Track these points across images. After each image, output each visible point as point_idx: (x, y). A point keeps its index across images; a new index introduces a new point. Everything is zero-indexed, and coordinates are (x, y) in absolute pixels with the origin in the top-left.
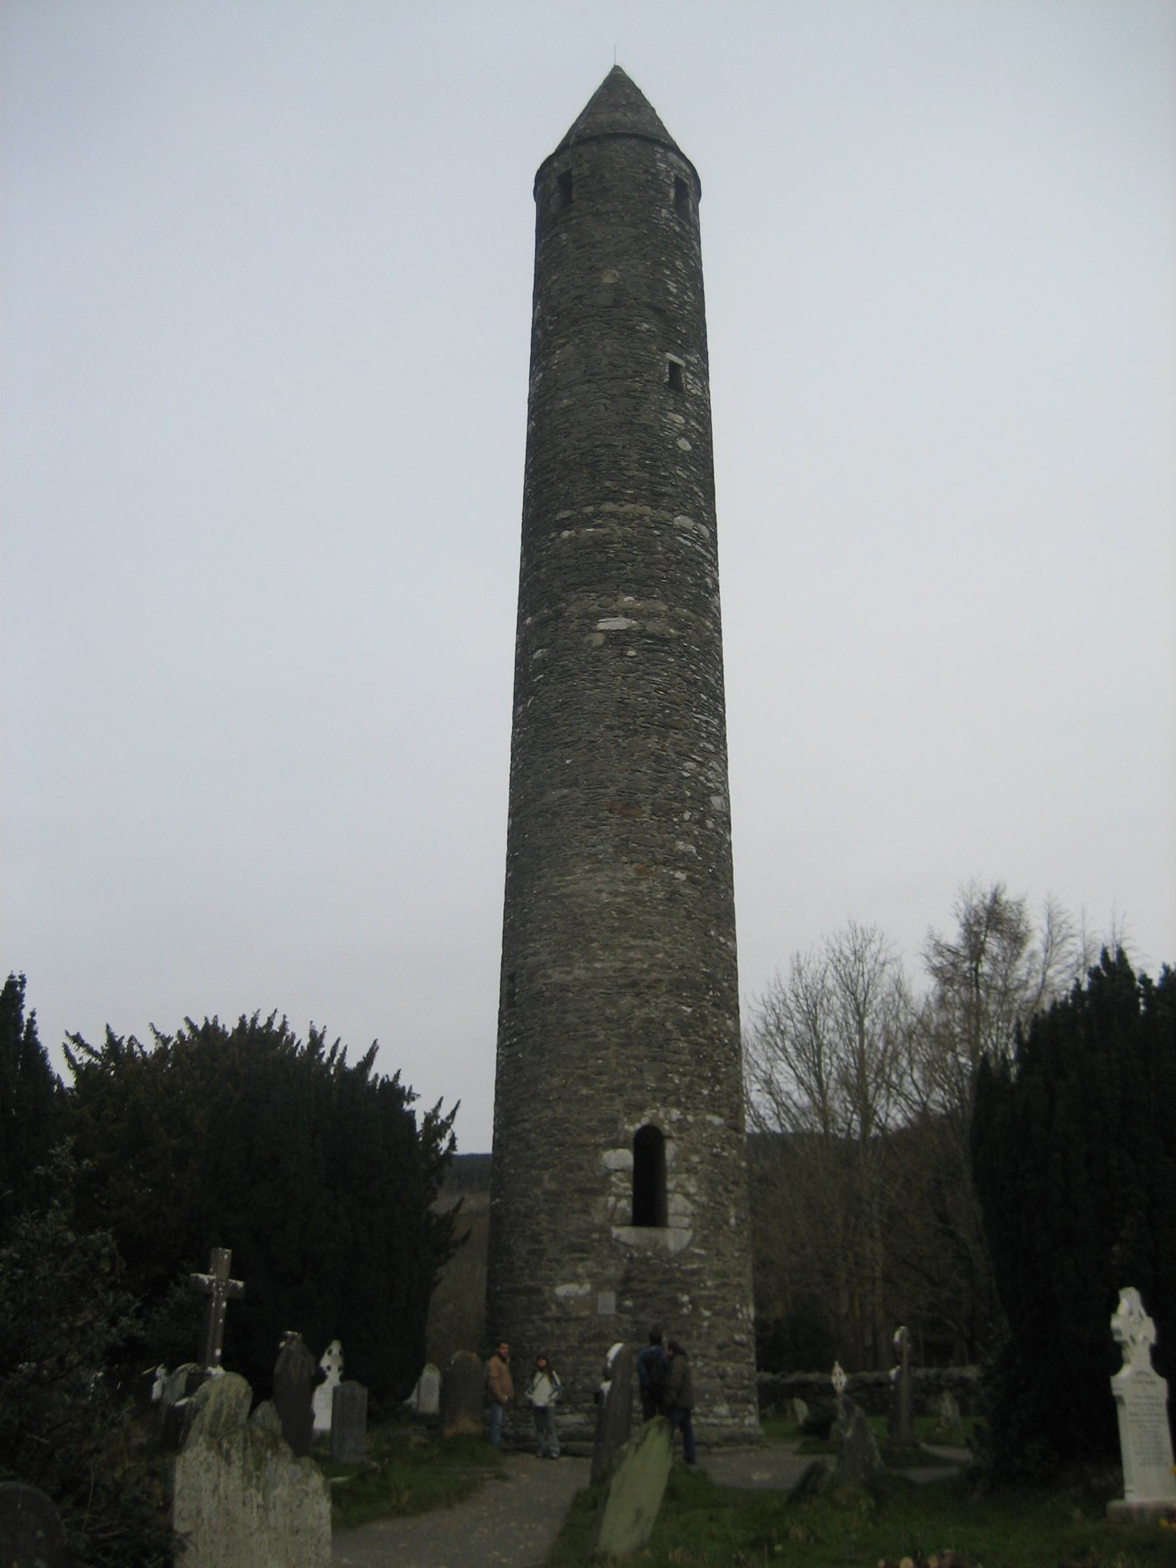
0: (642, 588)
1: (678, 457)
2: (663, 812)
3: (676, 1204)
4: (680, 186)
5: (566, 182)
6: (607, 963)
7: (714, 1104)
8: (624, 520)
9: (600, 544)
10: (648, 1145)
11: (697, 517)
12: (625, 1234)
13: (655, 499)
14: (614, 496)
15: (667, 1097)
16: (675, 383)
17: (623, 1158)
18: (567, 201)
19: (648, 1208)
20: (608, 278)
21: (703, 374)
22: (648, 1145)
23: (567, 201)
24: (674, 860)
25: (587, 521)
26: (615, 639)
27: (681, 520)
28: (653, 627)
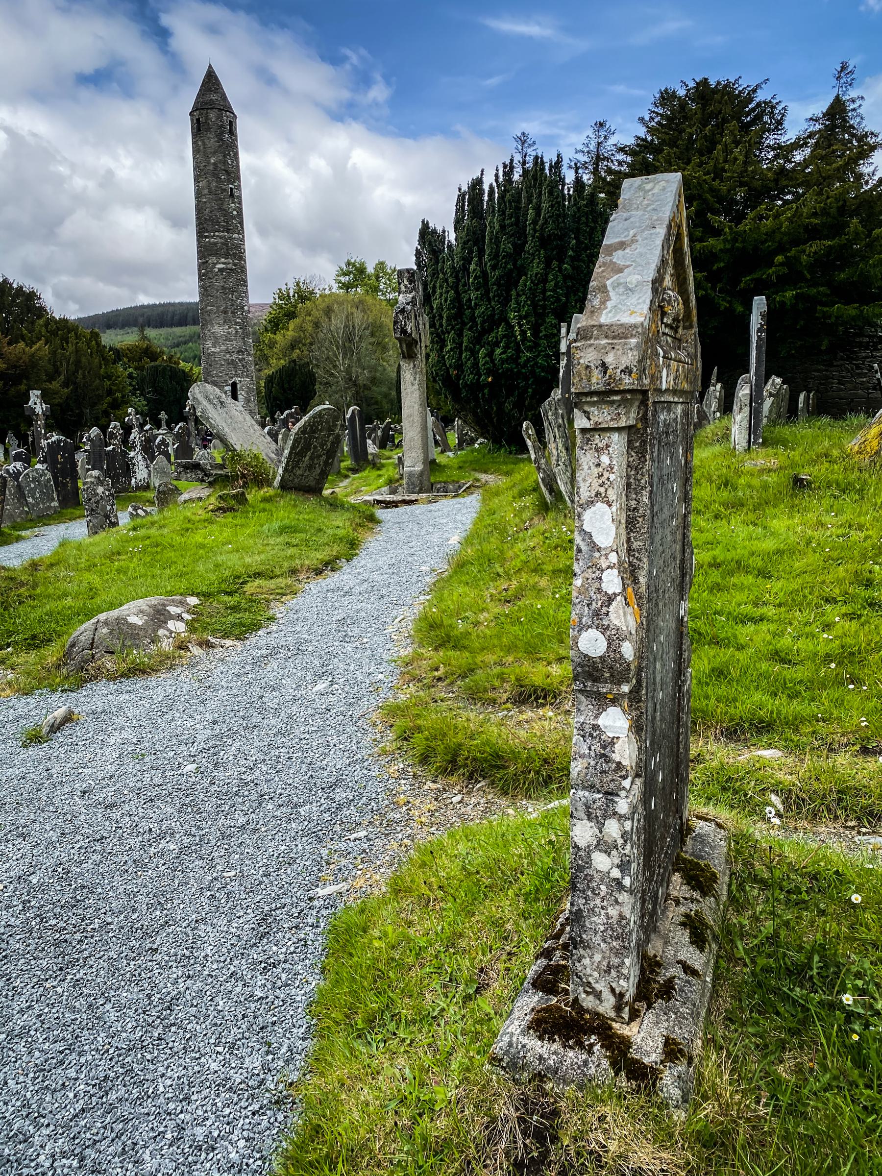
1: (233, 218)
2: (233, 313)
3: (240, 397)
4: (231, 123)
5: (198, 120)
7: (247, 376)
8: (221, 237)
9: (215, 244)
10: (234, 385)
11: (239, 233)
13: (228, 231)
16: (232, 195)
18: (199, 129)
21: (239, 188)
22: (234, 385)
25: (212, 237)
26: (220, 270)
27: (236, 236)
28: (229, 266)
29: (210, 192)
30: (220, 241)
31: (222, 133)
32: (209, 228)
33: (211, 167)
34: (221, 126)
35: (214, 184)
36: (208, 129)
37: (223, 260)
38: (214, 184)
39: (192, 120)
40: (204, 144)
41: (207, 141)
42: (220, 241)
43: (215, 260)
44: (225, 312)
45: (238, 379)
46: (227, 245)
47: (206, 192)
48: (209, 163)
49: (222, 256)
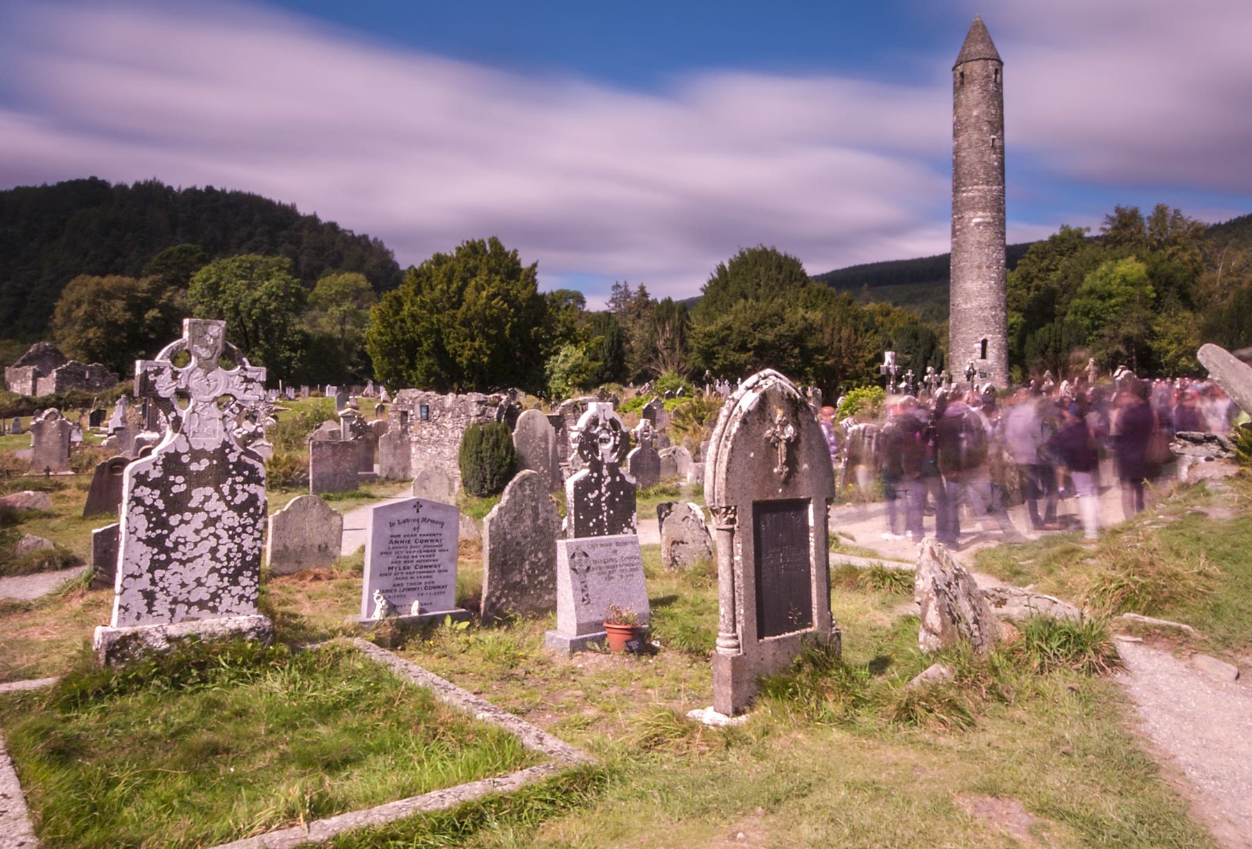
0: (984, 209)
2: (989, 267)
5: (962, 74)
6: (975, 304)
9: (973, 198)
10: (984, 343)
12: (979, 361)
13: (988, 183)
14: (977, 184)
15: (988, 332)
17: (980, 345)
19: (984, 356)
20: (975, 113)
22: (984, 343)
23: (962, 83)
24: (991, 279)
26: (978, 225)
29: (970, 146)
30: (977, 194)
31: (987, 83)
32: (968, 182)
33: (973, 120)
34: (988, 76)
35: (975, 136)
36: (972, 82)
37: (980, 213)
38: (975, 136)
39: (955, 75)
40: (967, 97)
41: (970, 94)
42: (977, 194)
43: (971, 214)
44: (979, 267)
45: (988, 337)
46: (985, 198)
47: (966, 145)
48: (970, 116)
49: (979, 209)
